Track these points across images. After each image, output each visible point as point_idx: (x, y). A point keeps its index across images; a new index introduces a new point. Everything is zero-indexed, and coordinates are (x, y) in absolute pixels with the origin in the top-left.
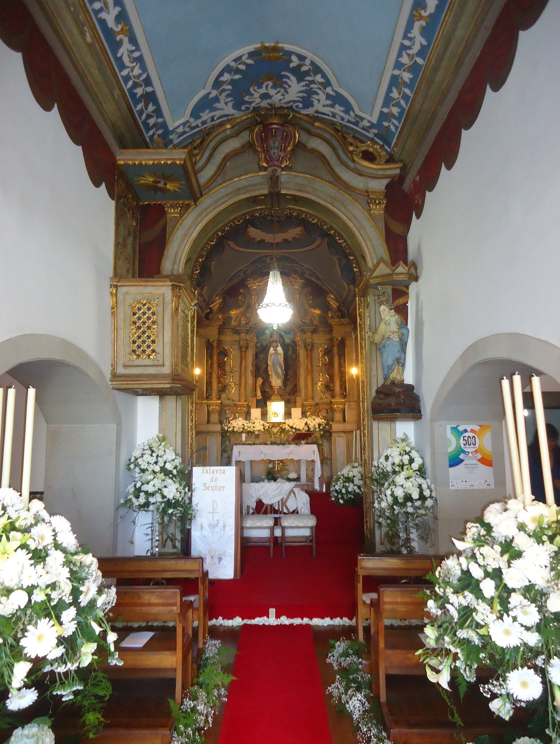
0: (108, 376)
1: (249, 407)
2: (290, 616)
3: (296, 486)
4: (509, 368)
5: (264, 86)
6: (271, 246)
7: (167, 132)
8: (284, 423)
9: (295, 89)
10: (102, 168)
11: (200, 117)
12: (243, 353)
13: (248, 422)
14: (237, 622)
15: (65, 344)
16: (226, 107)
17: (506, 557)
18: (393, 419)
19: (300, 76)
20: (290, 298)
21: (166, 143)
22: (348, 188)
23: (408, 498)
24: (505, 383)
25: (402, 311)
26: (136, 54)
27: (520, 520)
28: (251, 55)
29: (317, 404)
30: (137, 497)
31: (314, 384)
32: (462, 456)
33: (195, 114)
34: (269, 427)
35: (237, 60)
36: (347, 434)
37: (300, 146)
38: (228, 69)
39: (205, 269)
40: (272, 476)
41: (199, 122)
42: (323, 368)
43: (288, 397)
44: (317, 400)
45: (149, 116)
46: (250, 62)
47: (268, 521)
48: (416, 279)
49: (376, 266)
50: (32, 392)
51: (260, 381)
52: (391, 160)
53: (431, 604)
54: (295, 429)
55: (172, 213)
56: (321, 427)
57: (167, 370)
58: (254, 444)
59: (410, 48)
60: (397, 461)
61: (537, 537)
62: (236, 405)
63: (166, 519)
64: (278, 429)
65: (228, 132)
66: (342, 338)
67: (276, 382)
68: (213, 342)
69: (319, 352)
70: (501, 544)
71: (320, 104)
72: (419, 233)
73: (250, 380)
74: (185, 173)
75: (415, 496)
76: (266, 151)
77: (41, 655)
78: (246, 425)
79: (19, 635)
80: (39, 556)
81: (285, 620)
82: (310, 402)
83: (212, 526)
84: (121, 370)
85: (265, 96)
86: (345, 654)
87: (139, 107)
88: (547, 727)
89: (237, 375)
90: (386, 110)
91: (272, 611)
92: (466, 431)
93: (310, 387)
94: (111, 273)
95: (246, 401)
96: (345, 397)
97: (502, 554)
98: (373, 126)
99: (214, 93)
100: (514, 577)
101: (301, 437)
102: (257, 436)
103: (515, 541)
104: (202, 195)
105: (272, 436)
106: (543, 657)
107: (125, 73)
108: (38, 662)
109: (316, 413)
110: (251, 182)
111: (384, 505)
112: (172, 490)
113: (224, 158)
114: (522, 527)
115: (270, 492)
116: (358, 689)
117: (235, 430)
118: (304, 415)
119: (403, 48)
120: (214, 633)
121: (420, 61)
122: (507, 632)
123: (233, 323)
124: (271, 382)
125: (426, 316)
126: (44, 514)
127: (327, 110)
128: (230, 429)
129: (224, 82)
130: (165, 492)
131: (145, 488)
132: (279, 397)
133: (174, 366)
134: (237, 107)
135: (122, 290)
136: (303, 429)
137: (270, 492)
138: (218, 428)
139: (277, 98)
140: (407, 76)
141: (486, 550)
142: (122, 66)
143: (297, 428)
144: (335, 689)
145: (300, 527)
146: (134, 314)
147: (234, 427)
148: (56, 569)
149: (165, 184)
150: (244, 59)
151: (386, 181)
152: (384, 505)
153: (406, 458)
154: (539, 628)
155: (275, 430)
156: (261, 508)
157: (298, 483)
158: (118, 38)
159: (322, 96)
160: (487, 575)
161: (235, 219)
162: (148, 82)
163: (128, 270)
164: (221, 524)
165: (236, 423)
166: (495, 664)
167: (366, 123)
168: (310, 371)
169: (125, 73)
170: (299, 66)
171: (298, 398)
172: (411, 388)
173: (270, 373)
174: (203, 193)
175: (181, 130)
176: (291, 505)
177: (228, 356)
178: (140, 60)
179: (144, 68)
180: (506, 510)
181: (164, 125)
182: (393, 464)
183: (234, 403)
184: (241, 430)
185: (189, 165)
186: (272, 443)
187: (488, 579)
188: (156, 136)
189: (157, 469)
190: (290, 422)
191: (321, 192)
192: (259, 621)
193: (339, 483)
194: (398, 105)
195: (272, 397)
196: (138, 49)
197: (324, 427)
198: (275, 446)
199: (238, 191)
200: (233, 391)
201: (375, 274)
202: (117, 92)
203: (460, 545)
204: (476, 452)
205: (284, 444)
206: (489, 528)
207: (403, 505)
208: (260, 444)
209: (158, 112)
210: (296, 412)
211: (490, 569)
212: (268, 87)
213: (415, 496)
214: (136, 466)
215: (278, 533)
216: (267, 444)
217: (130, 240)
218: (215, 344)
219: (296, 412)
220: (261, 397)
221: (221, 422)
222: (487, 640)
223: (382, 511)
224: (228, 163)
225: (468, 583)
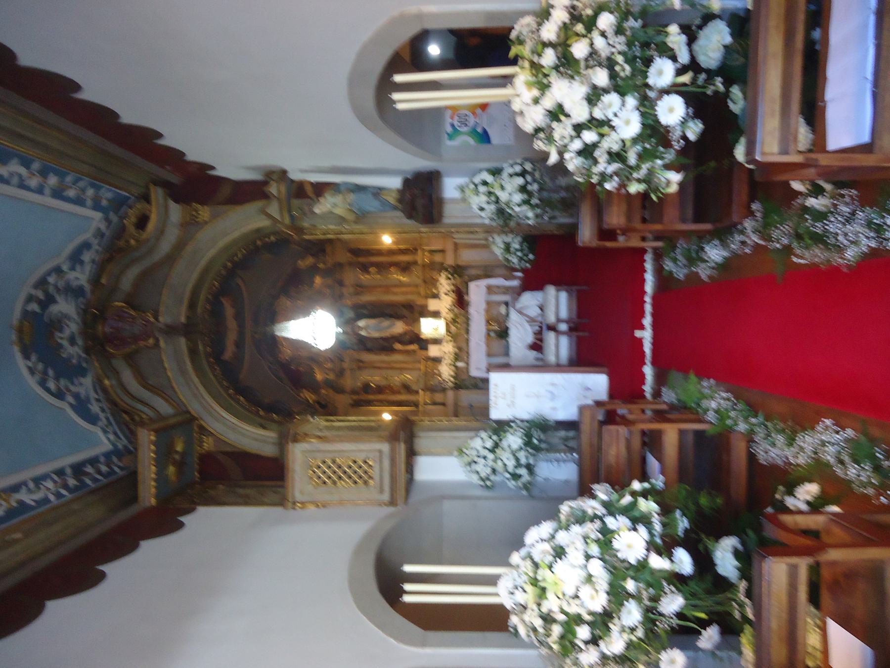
0: (392, 509)
1: (429, 359)
2: (642, 314)
3: (514, 307)
4: (385, 86)
5: (59, 341)
6: (241, 333)
7: (116, 452)
9: (65, 307)
10: (165, 520)
11: (98, 415)
14: (648, 371)
15: (359, 550)
16: (86, 385)
17: (562, 118)
18: (440, 202)
19: (50, 300)
20: (305, 311)
21: (130, 452)
22: (179, 247)
23: (523, 189)
24: (400, 106)
25: (320, 189)
26: (31, 485)
27: (529, 101)
28: (27, 357)
29: (425, 282)
30: (520, 476)
31: (401, 284)
32: (479, 130)
33: (92, 419)
35: (32, 371)
37: (130, 302)
38: (43, 384)
39: (271, 408)
40: (504, 334)
41: (102, 416)
44: (419, 281)
45: (99, 472)
46: (34, 358)
47: (550, 338)
48: (284, 172)
49: (269, 216)
50: (408, 568)
51: (398, 346)
52: (146, 198)
53: (608, 186)
55: (208, 445)
57: (385, 447)
59: (20, 176)
60: (484, 198)
61: (544, 87)
63: (543, 446)
65: (114, 382)
67: (399, 327)
69: (364, 278)
70: (552, 121)
71: (80, 277)
72: (232, 166)
74: (164, 432)
75: (520, 181)
76: (136, 339)
77: (644, 544)
79: (626, 565)
80: (560, 553)
81: (647, 321)
82: (422, 290)
83: (553, 396)
84: (386, 497)
85: (72, 341)
86: (675, 260)
87: (88, 482)
88: (705, 93)
89: (390, 372)
90: (89, 202)
91: (638, 334)
92: (453, 126)
93: (404, 289)
94: (278, 510)
96: (416, 250)
97: (559, 120)
98: (107, 220)
99: (70, 399)
100: (580, 112)
101: (461, 301)
102: (460, 349)
103: (548, 108)
104: (188, 412)
106: (647, 91)
107: (52, 498)
108: (651, 546)
109: (434, 282)
110: (173, 358)
111: (530, 214)
112: (514, 440)
113: (144, 387)
114: (536, 101)
115: (520, 335)
116: (702, 249)
118: (436, 296)
119: (22, 186)
120: (657, 394)
121: (36, 166)
122: (627, 122)
123: (331, 376)
125: (327, 163)
126: (523, 552)
127: (88, 268)
129: (59, 389)
130: (515, 446)
131: (511, 468)
133: (381, 439)
134: (83, 372)
135: (298, 496)
137: (520, 335)
138: (450, 394)
139: (73, 327)
140: (53, 180)
141: (556, 136)
142: (46, 500)
144: (704, 272)
145: (557, 303)
146: (325, 483)
148: (572, 538)
149: (177, 452)
150: (30, 364)
151: (172, 204)
152: (530, 214)
153: (482, 189)
154: (622, 94)
155: (453, 329)
156: (537, 346)
157: (510, 303)
158: (15, 504)
159: (72, 275)
160: (579, 136)
161: (214, 375)
162: (60, 473)
163: (275, 492)
164: (551, 388)
166: (654, 132)
167: (103, 227)
168: (387, 289)
169: (52, 498)
170: (40, 302)
171: (418, 303)
172: (407, 182)
174: (185, 409)
175: (112, 437)
176: (534, 312)
178: (38, 481)
179: (45, 477)
180: (521, 113)
181: (107, 455)
182: (488, 203)
184: (453, 368)
185: (156, 426)
186: (467, 331)
187: (581, 135)
188: (121, 464)
189: (491, 456)
190: (444, 312)
191: (185, 277)
192: (647, 348)
193: (510, 258)
194: (83, 190)
196: (25, 483)
199: (183, 372)
201: (279, 218)
202: (75, 506)
203: (553, 158)
204: (474, 113)
205: (468, 319)
206: (538, 130)
207: (530, 194)
209: (93, 461)
210: (433, 305)
211: (573, 133)
212: (62, 338)
213: (520, 181)
214: (488, 479)
215: (563, 327)
217: (241, 491)
218: (355, 397)
219: (433, 305)
222: (635, 141)
223: (537, 216)
224: (150, 382)
225: (587, 152)
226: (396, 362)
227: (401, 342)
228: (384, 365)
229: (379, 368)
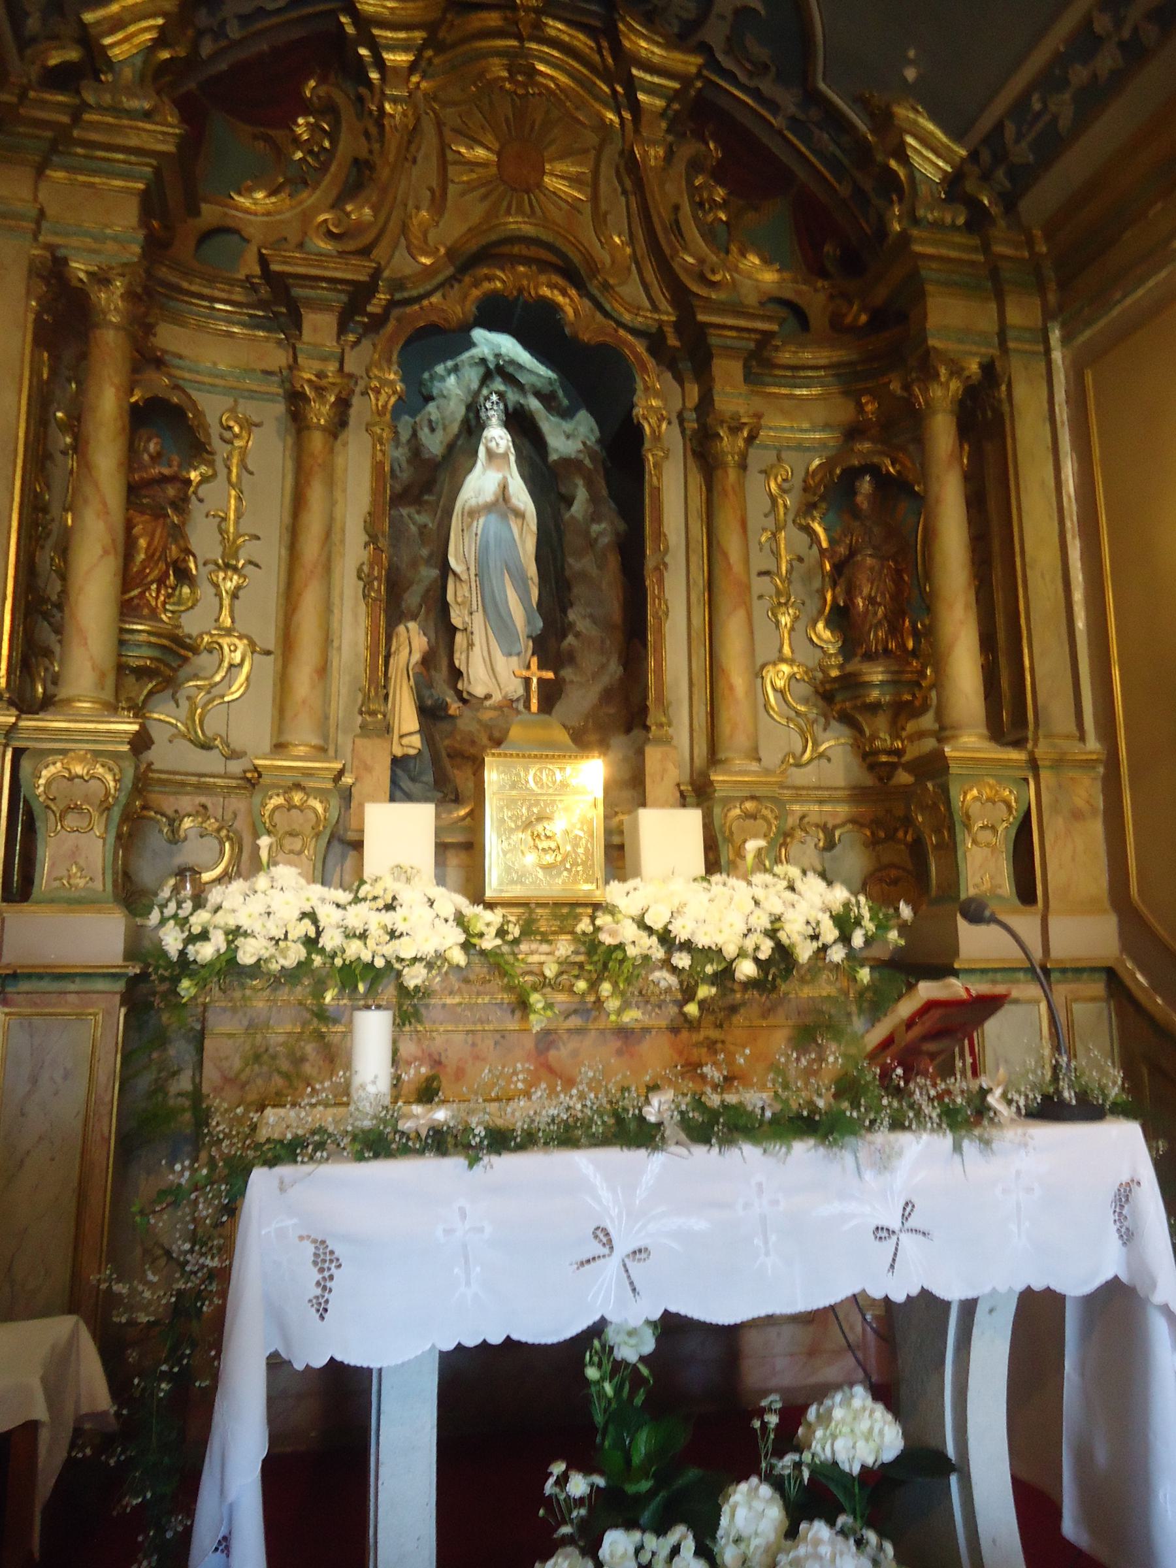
8: (597, 906)
13: (344, 897)
34: (501, 933)
36: (1061, 991)
42: (797, 591)
51: (413, 641)
54: (687, 946)
56: (858, 940)
58: (501, 1141)
62: (252, 782)
64: (564, 947)
66: (988, 369)
67: (495, 668)
68: (102, 279)
73: (353, 627)
78: (329, 916)
89: (265, 585)
95: (321, 751)
105: (536, 999)
117: (246, 956)
118: (717, 857)
124: (456, 674)
128: (205, 952)
132: (563, 737)
136: (742, 953)
138: (101, 938)
143: (702, 941)
147: (235, 933)
165: (257, 905)
171: (653, 756)
173: (457, 618)
177: (211, 464)
183: (236, 767)
184: (295, 954)
186: (712, 1126)
195: (515, 732)
197: (869, 941)
198: (748, 1153)
200: (236, 691)
208: (567, 1135)
216: (636, 1133)
218: (111, 302)
219: (670, 835)
220: (416, 741)
221: (132, 896)
226: (327, 609)
227: (427, 661)
228: (311, 548)
229: (298, 502)
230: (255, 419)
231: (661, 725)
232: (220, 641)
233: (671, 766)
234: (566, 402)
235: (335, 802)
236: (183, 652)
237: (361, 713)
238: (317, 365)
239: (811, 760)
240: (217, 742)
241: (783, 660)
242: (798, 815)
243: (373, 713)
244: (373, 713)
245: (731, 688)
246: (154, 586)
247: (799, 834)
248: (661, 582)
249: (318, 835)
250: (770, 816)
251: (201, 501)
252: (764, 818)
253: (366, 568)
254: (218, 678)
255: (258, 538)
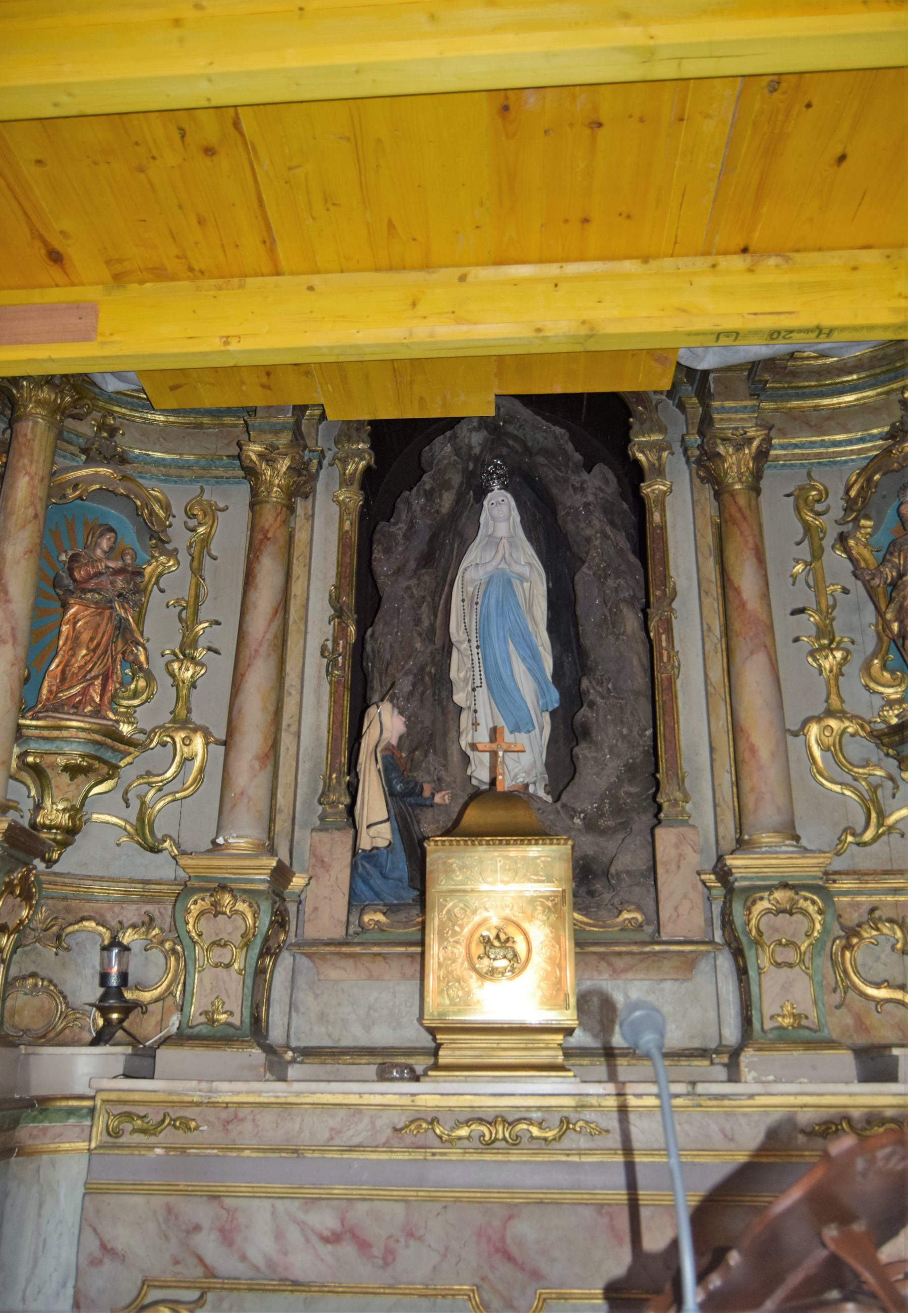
12: (269, 517)
43: (590, 844)
173: (459, 698)
230: (221, 505)
231: (675, 803)
232: (173, 734)
233: (688, 850)
234: (578, 457)
235: (266, 907)
236: (122, 747)
237: (321, 804)
238: (269, 438)
239: (875, 839)
240: (167, 844)
241: (830, 713)
242: (865, 909)
243: (333, 804)
244: (333, 804)
245: (753, 750)
246: (98, 682)
247: (868, 933)
248: (669, 631)
249: (247, 945)
250: (811, 909)
251: (162, 591)
252: (804, 912)
253: (330, 644)
254: (169, 774)
255: (218, 623)
